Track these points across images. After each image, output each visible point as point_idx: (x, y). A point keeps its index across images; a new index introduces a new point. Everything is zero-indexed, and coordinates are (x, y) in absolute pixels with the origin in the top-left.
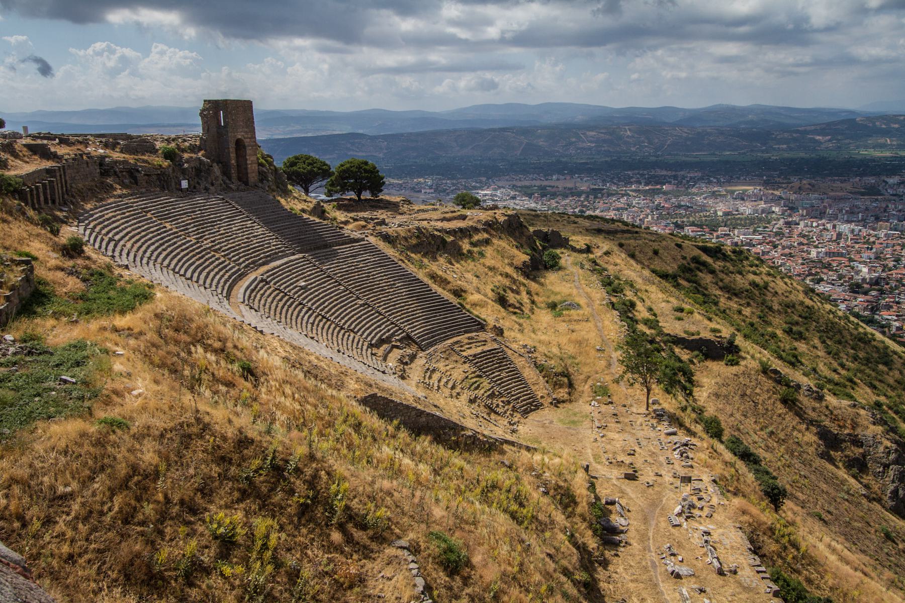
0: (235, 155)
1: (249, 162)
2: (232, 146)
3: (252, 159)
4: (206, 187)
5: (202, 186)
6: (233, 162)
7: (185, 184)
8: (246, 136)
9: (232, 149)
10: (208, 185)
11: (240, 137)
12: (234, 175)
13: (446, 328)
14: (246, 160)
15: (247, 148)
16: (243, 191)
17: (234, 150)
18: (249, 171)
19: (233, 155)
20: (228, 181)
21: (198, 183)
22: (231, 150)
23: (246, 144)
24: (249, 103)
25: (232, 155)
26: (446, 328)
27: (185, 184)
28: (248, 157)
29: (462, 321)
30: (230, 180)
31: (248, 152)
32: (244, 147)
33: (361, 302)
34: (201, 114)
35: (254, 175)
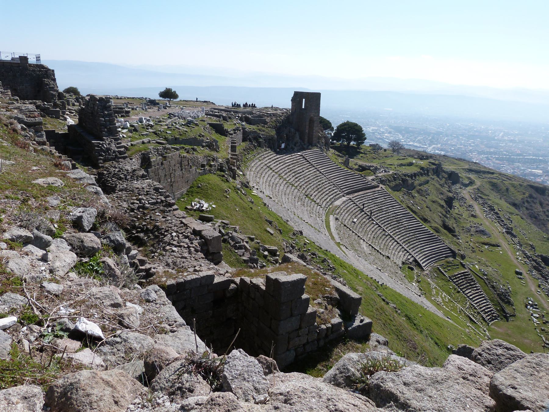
1: (314, 131)
5: (291, 146)
6: (307, 131)
7: (283, 146)
9: (307, 123)
10: (293, 146)
11: (312, 116)
12: (306, 140)
13: (434, 254)
18: (314, 137)
19: (307, 127)
20: (302, 143)
26: (434, 254)
27: (283, 146)
29: (443, 249)
31: (315, 125)
34: (292, 100)
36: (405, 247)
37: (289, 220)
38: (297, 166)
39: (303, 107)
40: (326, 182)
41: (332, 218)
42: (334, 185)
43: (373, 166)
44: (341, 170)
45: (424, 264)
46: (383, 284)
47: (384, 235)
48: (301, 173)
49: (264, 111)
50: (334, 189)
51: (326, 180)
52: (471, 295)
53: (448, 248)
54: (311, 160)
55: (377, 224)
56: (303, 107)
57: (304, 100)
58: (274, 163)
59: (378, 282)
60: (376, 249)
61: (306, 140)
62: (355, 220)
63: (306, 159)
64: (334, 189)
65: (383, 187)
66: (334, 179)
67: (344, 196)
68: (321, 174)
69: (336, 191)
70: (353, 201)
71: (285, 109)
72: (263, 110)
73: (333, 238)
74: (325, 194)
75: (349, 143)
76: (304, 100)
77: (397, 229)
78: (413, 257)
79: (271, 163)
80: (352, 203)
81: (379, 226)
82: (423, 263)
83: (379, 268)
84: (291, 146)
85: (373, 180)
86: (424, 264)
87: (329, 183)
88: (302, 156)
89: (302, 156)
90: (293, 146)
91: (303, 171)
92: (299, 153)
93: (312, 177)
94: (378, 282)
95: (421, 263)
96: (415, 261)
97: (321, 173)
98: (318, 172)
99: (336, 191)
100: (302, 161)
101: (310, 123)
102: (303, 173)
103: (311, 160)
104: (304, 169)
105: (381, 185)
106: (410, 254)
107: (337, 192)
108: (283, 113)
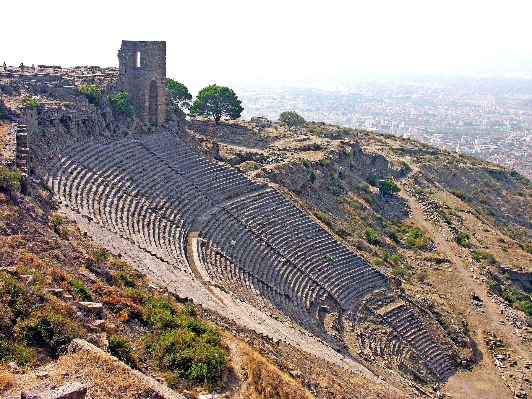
1: (159, 103)
2: (147, 87)
3: (161, 100)
4: (124, 131)
5: (121, 130)
6: (147, 103)
8: (159, 77)
9: (147, 92)
10: (126, 129)
11: (154, 78)
14: (157, 102)
16: (155, 132)
17: (149, 92)
18: (159, 112)
19: (147, 97)
20: (141, 124)
21: (117, 127)
22: (146, 92)
23: (158, 85)
24: (164, 43)
25: (146, 97)
32: (156, 88)
33: (284, 260)
34: (119, 55)
35: (162, 115)
37: (122, 254)
38: (133, 163)
39: (139, 65)
40: (182, 184)
42: (196, 188)
43: (257, 154)
44: (206, 163)
45: (343, 302)
46: (280, 340)
47: (280, 262)
48: (141, 172)
49: (74, 74)
50: (196, 194)
51: (183, 181)
52: (413, 339)
53: (377, 272)
54: (155, 150)
55: (269, 246)
56: (139, 65)
57: (139, 54)
58: (96, 160)
59: (272, 339)
60: (270, 285)
61: (147, 118)
62: (234, 242)
63: (148, 150)
64: (196, 194)
65: (274, 185)
66: (195, 178)
67: (213, 205)
68: (173, 173)
69: (199, 198)
70: (228, 213)
71: (108, 68)
72: (73, 72)
73: (198, 276)
74: (182, 205)
75: (218, 119)
76: (139, 54)
77: (300, 251)
78: (325, 291)
79: (89, 161)
80: (226, 215)
81: (272, 249)
82: (341, 300)
83: (275, 316)
85: (258, 176)
86: (343, 302)
87: (188, 187)
88: (141, 144)
90: (126, 129)
91: (144, 170)
92: (136, 141)
93: (160, 179)
94: (272, 339)
95: (338, 300)
96: (330, 296)
97: (173, 170)
98: (169, 170)
99: (199, 198)
100: (141, 152)
101: (151, 91)
102: (146, 172)
103: (155, 150)
104: (146, 166)
105: (271, 184)
106: (321, 288)
107: (201, 200)
108: (106, 76)
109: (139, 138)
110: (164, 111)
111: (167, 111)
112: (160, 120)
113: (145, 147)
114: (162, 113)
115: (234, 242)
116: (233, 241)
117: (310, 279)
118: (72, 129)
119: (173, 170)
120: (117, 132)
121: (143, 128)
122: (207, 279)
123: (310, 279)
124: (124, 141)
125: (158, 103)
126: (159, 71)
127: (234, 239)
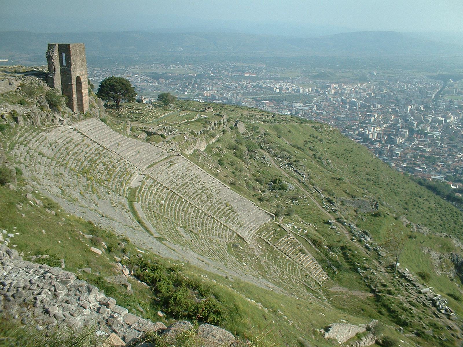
0: (76, 90)
1: (83, 95)
2: (74, 82)
4: (60, 120)
15: (83, 83)
18: (84, 102)
19: (74, 90)
23: (82, 80)
28: (83, 91)
30: (73, 111)
36: (223, 223)
41: (137, 206)
63: (82, 134)
68: (105, 151)
73: (151, 235)
84: (58, 119)
88: (75, 130)
89: (75, 130)
92: (71, 127)
106: (230, 229)
109: (73, 124)
110: (88, 101)
111: (90, 100)
112: (86, 108)
113: (79, 132)
114: (86, 103)
115: (162, 202)
116: (162, 201)
117: (221, 224)
118: (20, 121)
119: (105, 148)
120: (55, 121)
121: (74, 116)
122: (157, 235)
123: (221, 224)
124: (62, 128)
125: (83, 94)
126: (82, 68)
127: (162, 200)
